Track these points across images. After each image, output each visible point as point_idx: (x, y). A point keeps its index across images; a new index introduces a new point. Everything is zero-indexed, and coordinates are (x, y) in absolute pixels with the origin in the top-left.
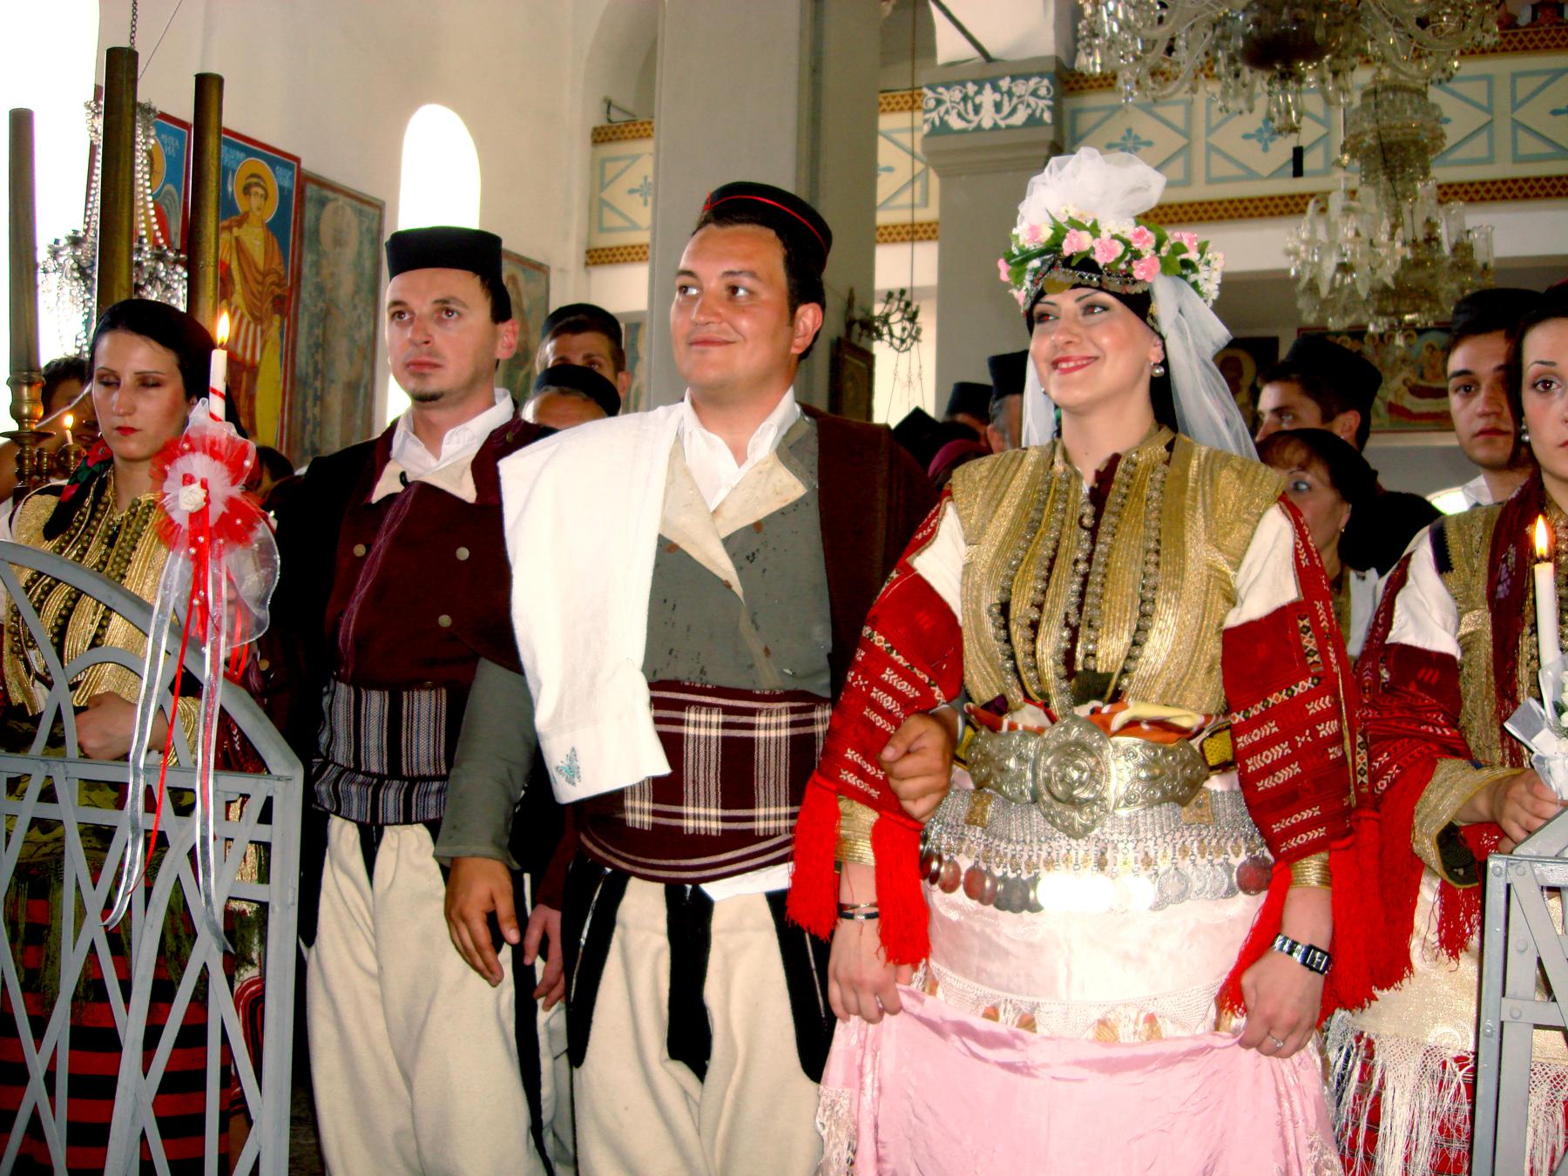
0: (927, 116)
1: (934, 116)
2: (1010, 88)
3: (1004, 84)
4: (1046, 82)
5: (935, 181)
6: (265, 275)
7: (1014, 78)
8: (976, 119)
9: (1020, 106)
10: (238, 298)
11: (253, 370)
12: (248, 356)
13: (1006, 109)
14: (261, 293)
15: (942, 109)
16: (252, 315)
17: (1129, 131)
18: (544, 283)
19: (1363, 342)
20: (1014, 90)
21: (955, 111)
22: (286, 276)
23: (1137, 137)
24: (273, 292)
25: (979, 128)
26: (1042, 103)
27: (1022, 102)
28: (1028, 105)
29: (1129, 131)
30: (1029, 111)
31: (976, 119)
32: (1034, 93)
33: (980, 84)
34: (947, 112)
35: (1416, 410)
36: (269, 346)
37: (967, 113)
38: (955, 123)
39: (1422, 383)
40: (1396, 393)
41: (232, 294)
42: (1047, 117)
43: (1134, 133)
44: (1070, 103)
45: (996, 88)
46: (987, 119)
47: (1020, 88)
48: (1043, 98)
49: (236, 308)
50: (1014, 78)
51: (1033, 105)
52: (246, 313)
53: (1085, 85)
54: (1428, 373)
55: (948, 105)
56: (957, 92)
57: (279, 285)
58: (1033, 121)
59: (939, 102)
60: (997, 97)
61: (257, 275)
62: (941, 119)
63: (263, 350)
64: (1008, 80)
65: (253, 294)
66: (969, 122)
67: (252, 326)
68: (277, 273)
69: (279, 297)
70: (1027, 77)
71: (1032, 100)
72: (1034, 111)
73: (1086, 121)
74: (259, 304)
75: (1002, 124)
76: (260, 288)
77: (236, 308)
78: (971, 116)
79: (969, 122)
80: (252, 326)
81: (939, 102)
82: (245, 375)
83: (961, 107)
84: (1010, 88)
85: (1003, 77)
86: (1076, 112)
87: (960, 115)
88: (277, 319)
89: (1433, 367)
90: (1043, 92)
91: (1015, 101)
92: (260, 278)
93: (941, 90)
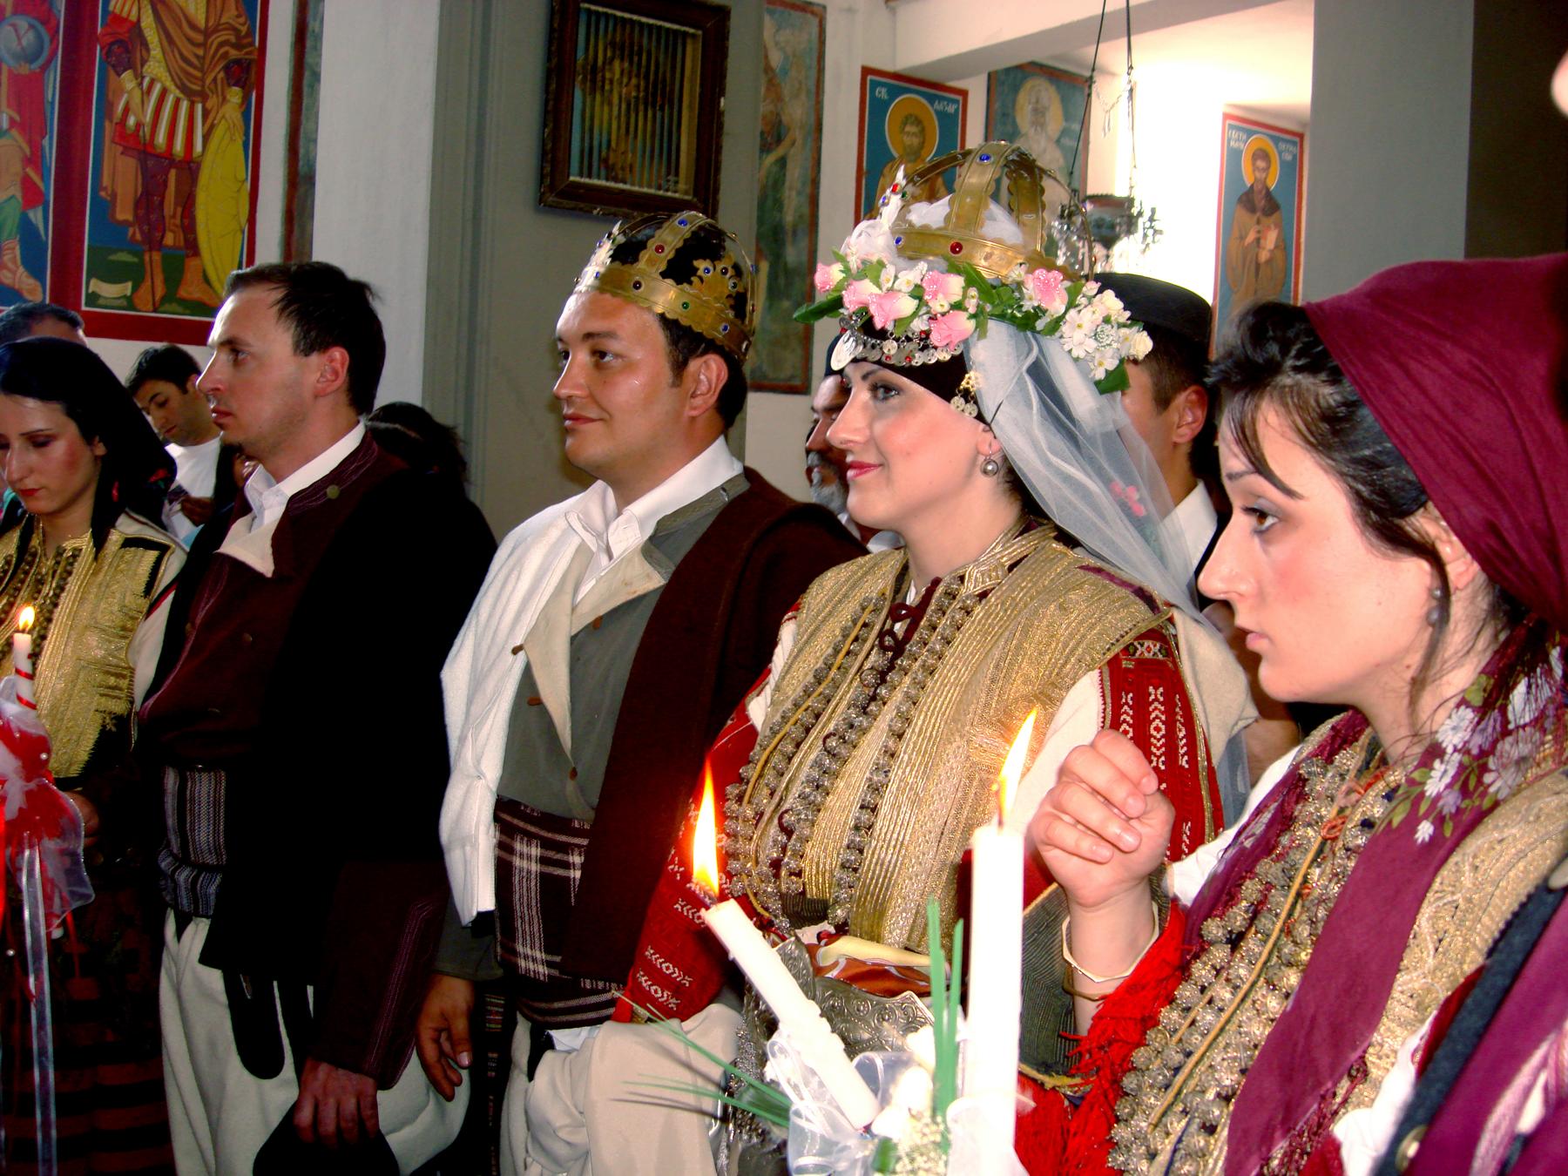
6: (207, 33)
10: (156, 66)
11: (190, 168)
12: (179, 146)
14: (201, 59)
16: (183, 88)
18: (815, 30)
22: (250, 33)
24: (227, 53)
36: (218, 133)
41: (144, 62)
49: (152, 82)
52: (169, 84)
57: (238, 46)
61: (192, 34)
63: (206, 138)
65: (185, 60)
67: (185, 105)
68: (235, 29)
69: (238, 62)
74: (199, 74)
76: (200, 52)
77: (152, 82)
80: (185, 105)
82: (173, 173)
88: (235, 95)
92: (199, 38)
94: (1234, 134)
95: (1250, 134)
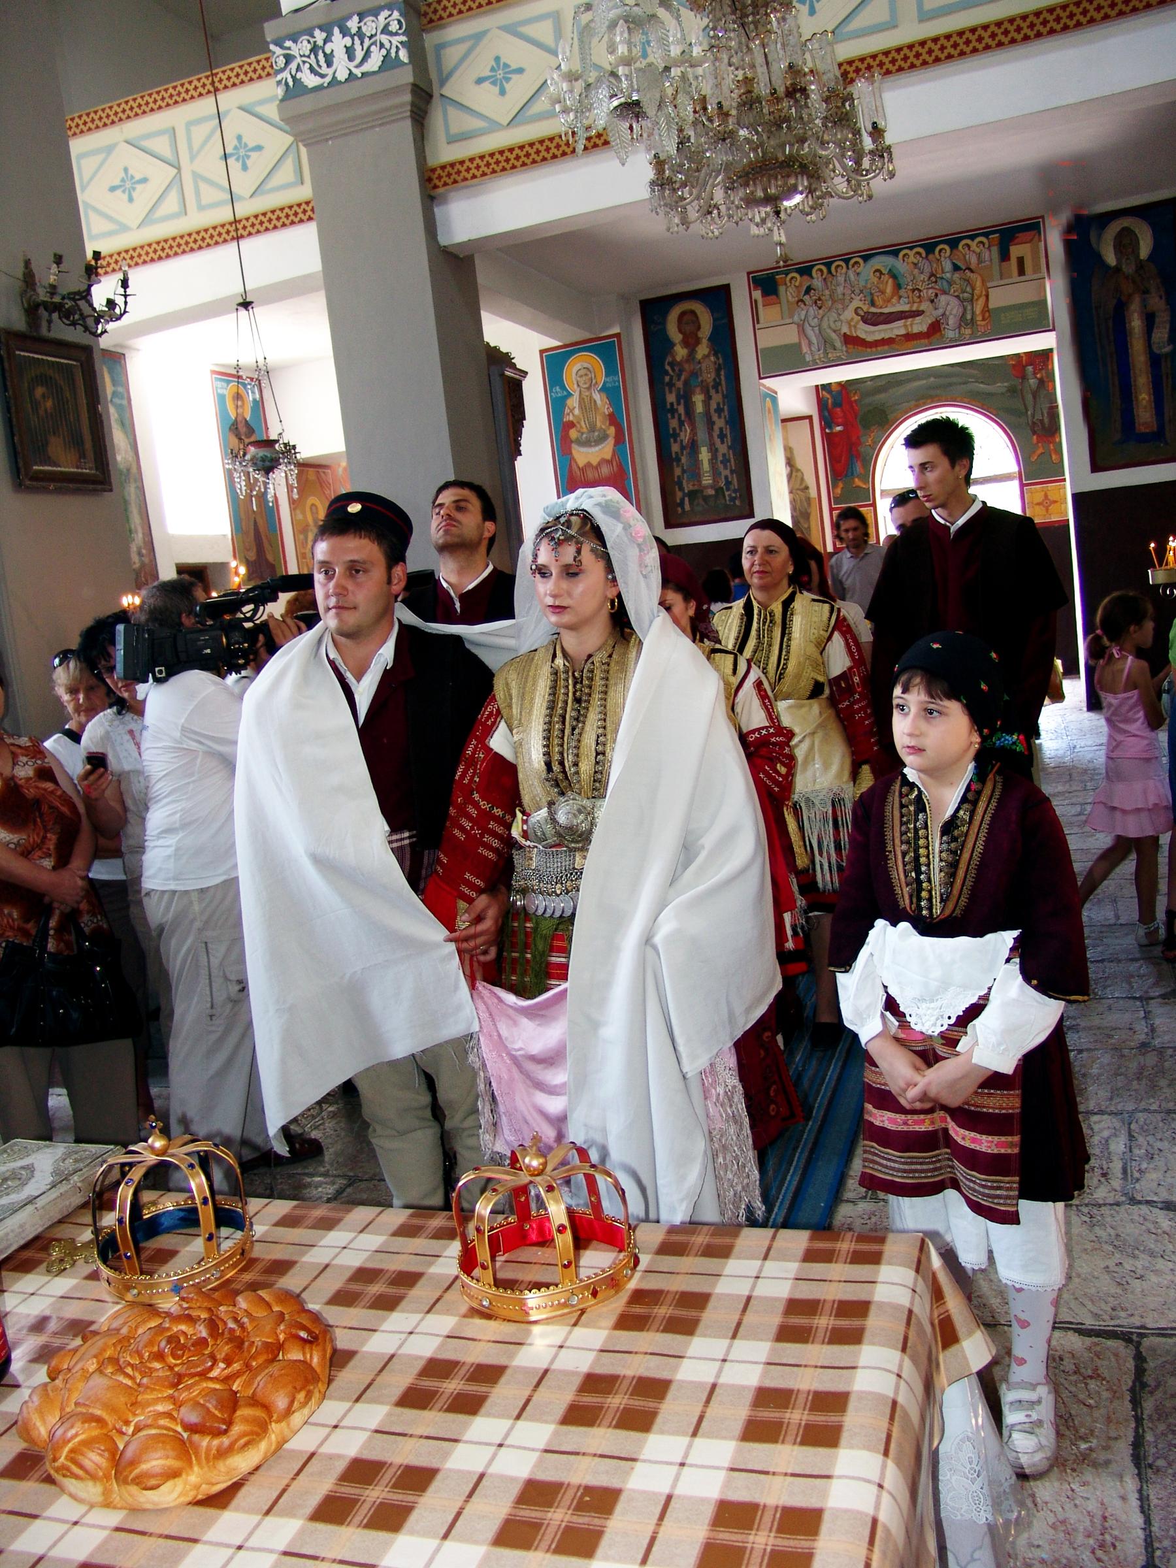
0: (279, 77)
1: (286, 75)
2: (359, 28)
3: (353, 24)
4: (396, 14)
5: (303, 151)
7: (362, 17)
8: (330, 71)
9: (373, 48)
13: (359, 54)
15: (293, 66)
17: (497, 59)
19: (812, 277)
20: (364, 29)
21: (307, 65)
23: (506, 66)
25: (334, 82)
26: (395, 40)
27: (374, 43)
28: (382, 46)
29: (497, 59)
30: (384, 52)
31: (330, 71)
32: (385, 30)
33: (327, 29)
34: (298, 69)
35: (869, 339)
37: (320, 67)
38: (311, 81)
39: (873, 310)
40: (849, 323)
42: (403, 55)
43: (503, 60)
44: (430, 39)
45: (345, 32)
46: (341, 68)
47: (369, 27)
48: (396, 34)
50: (362, 17)
51: (387, 45)
53: (445, 15)
54: (879, 301)
55: (299, 60)
56: (305, 43)
58: (388, 63)
59: (289, 59)
60: (348, 41)
62: (294, 77)
64: (356, 18)
66: (323, 76)
70: (375, 12)
71: (384, 39)
72: (388, 52)
73: (452, 55)
75: (358, 72)
78: (324, 70)
79: (323, 76)
81: (289, 59)
83: (312, 60)
84: (359, 28)
85: (349, 17)
86: (440, 47)
87: (312, 69)
89: (883, 292)
90: (394, 27)
91: (367, 42)
93: (288, 44)
94: (219, 384)
95: (228, 382)
